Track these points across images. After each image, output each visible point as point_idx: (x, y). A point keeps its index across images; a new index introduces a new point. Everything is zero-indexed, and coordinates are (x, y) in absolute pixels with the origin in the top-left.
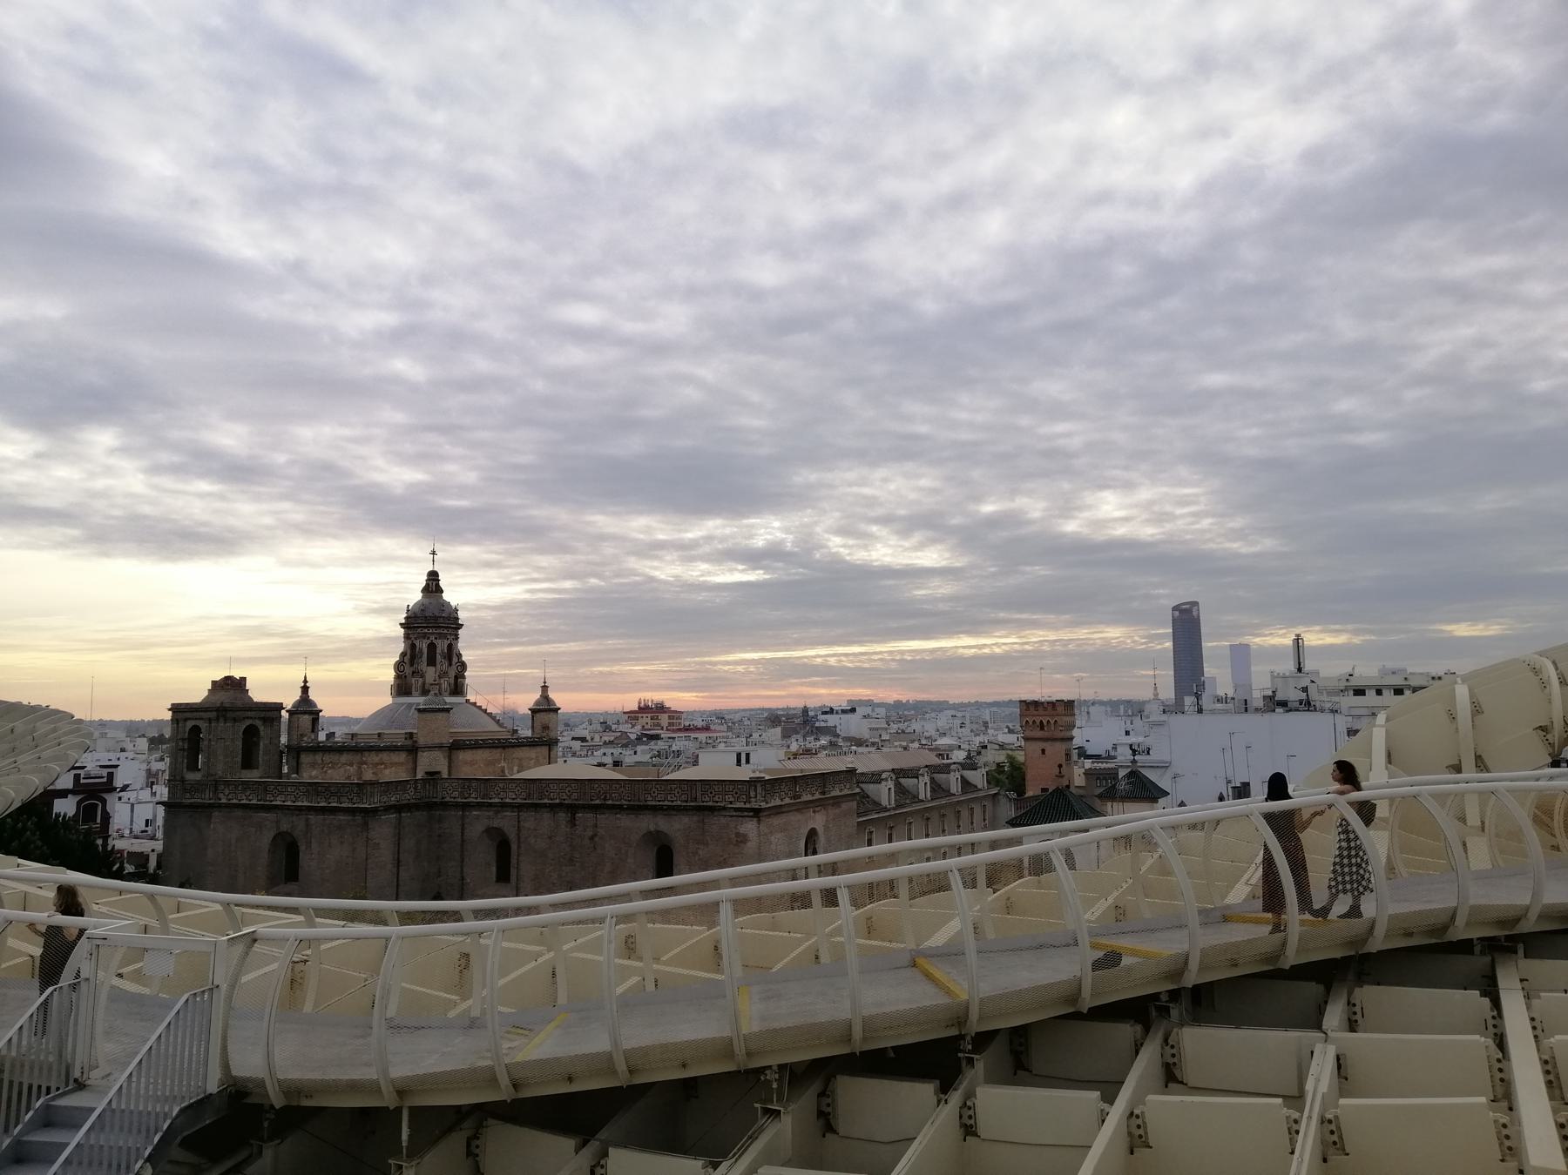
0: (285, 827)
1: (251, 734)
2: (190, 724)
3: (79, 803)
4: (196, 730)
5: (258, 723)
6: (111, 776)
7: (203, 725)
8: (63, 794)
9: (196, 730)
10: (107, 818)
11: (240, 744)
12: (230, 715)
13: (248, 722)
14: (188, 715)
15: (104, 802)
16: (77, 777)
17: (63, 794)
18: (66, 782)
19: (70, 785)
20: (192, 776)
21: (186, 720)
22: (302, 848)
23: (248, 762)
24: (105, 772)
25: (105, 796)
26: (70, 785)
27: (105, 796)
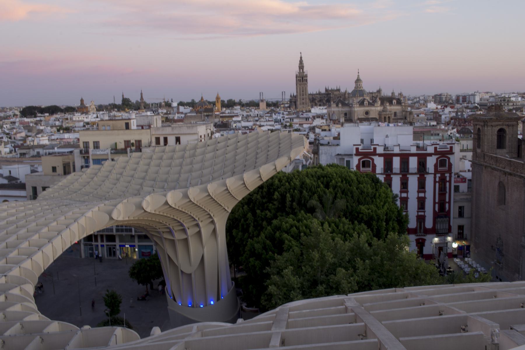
0: (502, 179)
1: (501, 133)
2: (478, 127)
3: (437, 159)
4: (479, 129)
5: (504, 127)
6: (451, 148)
7: (481, 128)
8: (430, 155)
9: (479, 129)
10: (450, 165)
11: (495, 137)
12: (489, 124)
13: (499, 127)
14: (477, 123)
15: (449, 158)
16: (436, 148)
17: (430, 155)
18: (431, 150)
19: (433, 152)
20: (479, 151)
21: (476, 125)
22: (506, 190)
23: (501, 144)
24: (449, 146)
25: (449, 156)
26: (433, 152)
27: (449, 156)
